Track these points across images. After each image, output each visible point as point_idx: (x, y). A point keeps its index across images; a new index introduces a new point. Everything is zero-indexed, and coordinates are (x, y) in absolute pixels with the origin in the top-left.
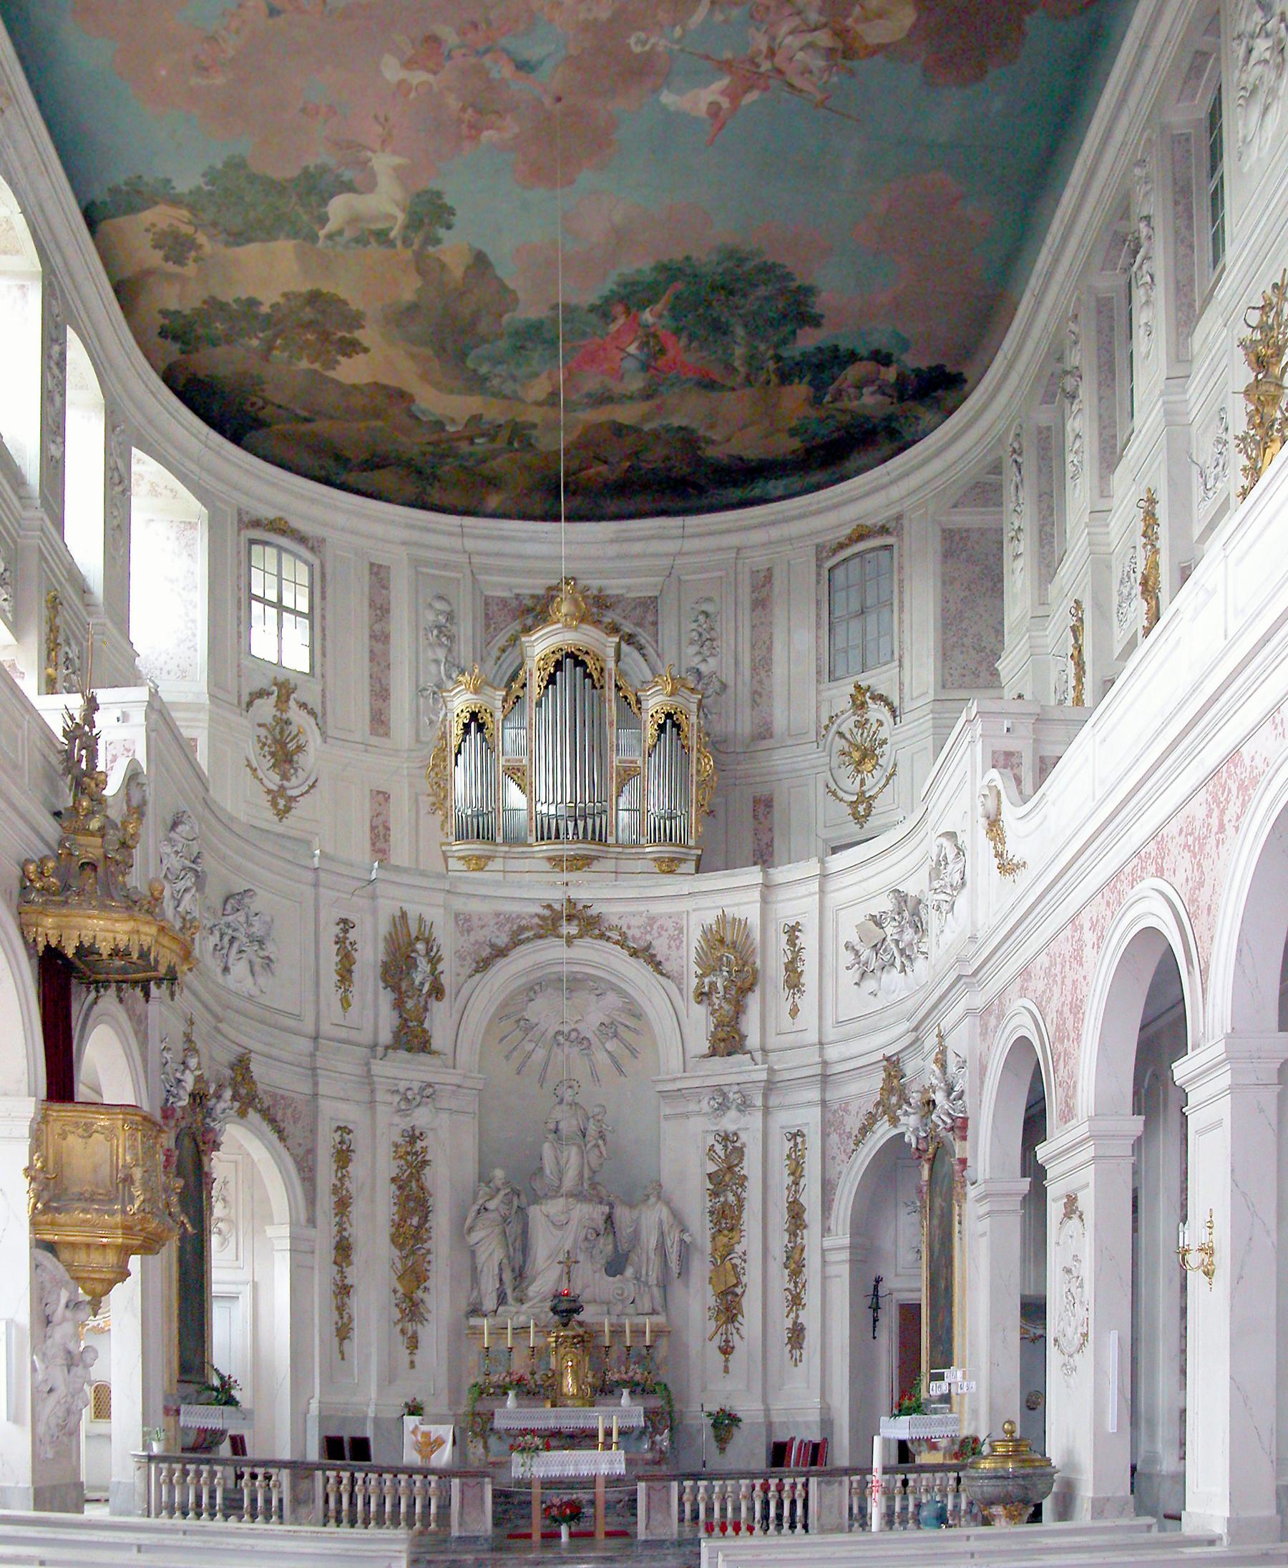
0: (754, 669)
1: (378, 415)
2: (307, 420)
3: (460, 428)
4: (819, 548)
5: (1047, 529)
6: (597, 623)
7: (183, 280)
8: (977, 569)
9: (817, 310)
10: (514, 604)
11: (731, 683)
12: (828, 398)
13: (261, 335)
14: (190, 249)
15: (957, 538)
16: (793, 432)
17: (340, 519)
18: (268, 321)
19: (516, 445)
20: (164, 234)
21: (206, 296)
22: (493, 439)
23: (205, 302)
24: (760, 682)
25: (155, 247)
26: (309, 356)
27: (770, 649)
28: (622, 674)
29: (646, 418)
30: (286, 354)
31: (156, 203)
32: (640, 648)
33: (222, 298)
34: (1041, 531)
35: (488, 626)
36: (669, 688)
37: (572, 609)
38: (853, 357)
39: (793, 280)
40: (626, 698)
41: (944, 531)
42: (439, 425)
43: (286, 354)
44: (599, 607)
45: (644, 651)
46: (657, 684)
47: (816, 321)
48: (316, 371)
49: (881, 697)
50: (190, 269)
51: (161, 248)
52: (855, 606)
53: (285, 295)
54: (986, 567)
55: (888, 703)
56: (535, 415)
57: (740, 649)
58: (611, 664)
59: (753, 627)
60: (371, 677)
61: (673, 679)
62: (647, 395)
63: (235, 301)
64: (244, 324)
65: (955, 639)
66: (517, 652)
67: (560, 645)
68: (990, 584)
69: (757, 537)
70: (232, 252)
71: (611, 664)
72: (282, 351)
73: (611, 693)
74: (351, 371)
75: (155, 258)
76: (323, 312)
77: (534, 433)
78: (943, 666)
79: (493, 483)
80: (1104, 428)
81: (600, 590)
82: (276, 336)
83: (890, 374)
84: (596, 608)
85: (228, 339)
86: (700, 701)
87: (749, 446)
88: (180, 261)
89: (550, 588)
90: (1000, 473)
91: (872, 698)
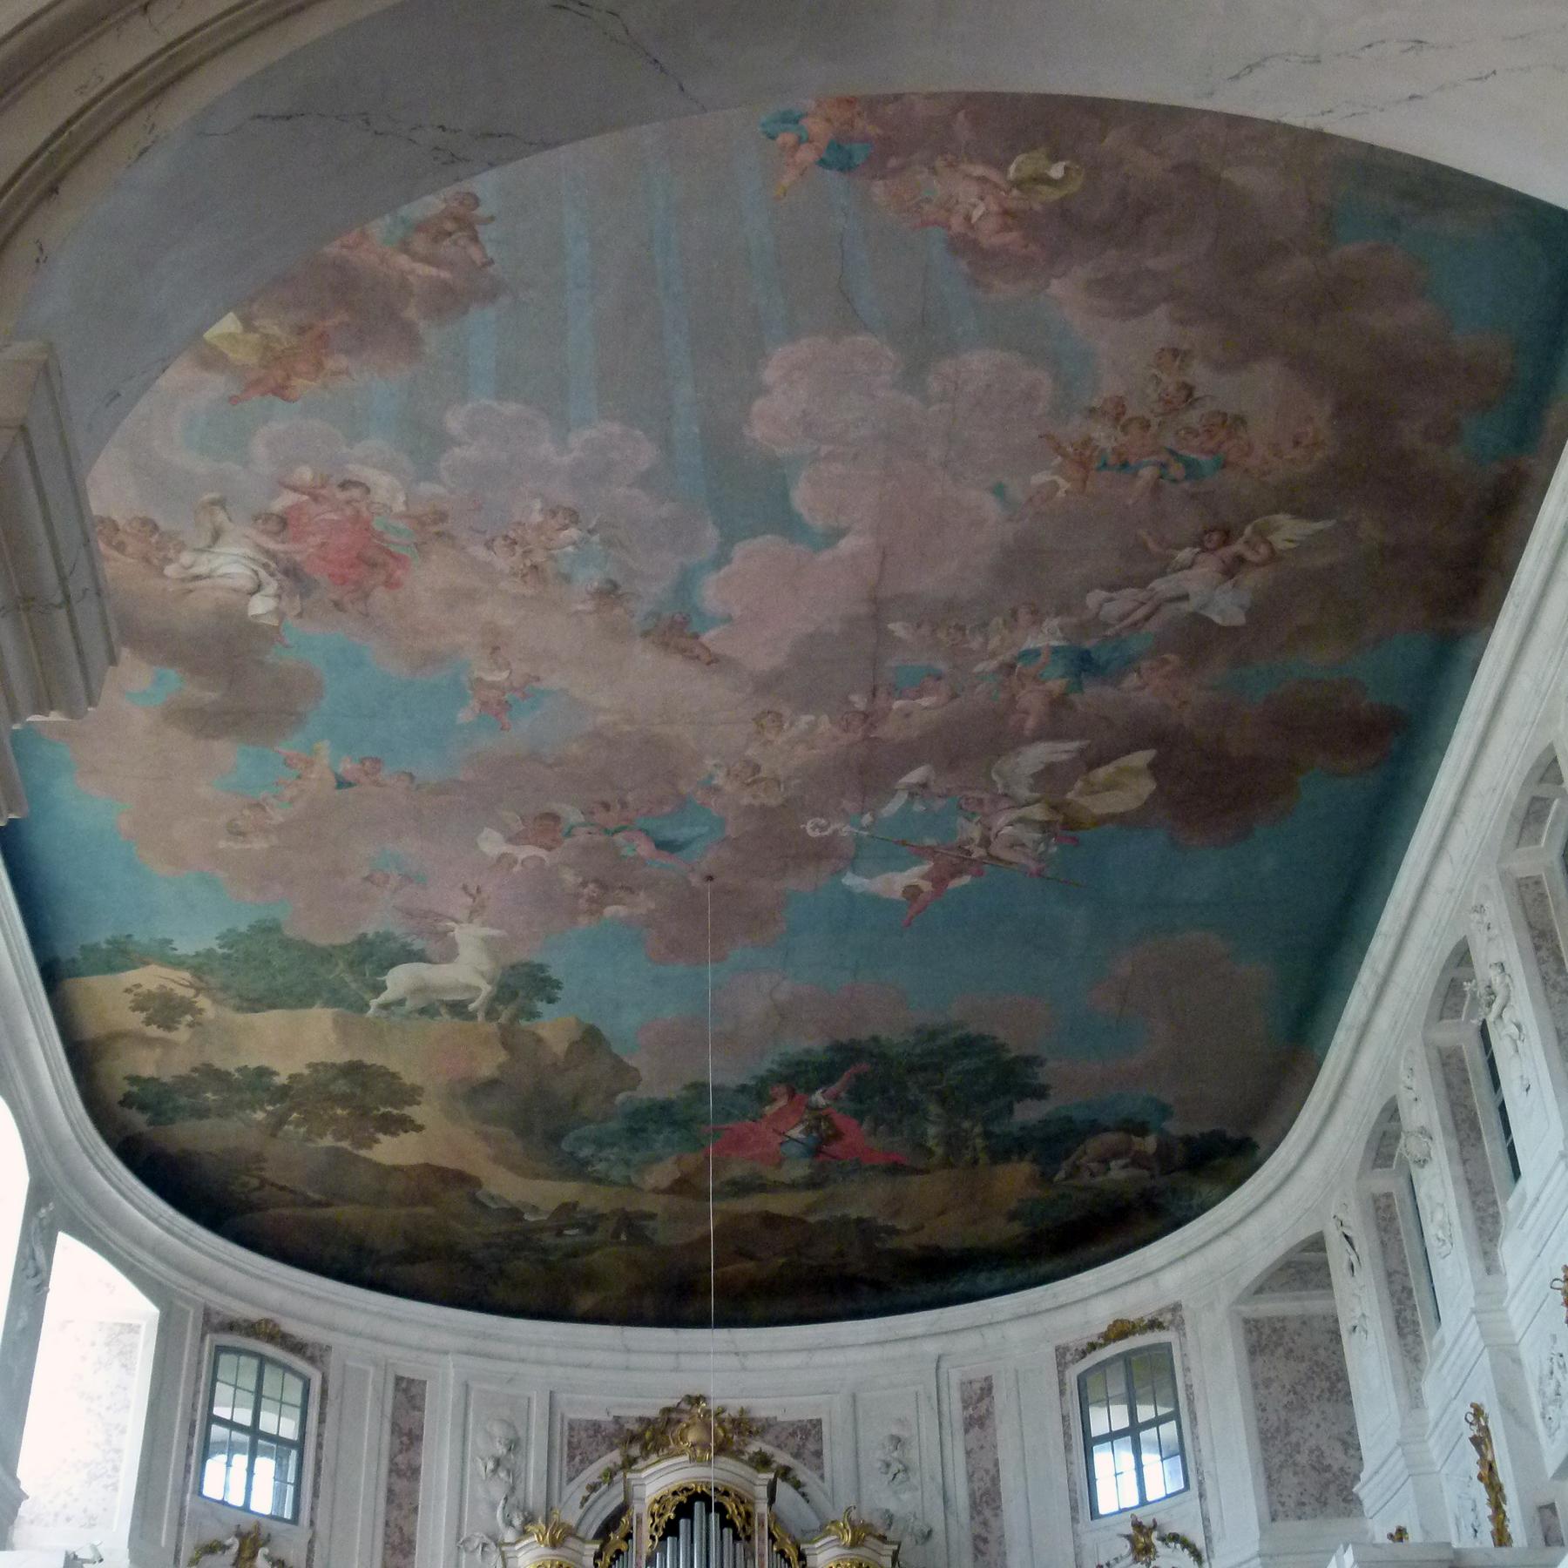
0: (975, 1507)
1: (426, 1199)
2: (328, 1205)
3: (545, 1218)
4: (1063, 1356)
5: (1408, 1314)
6: (737, 1455)
7: (166, 1044)
8: (1304, 1366)
9: (1043, 1076)
10: (612, 1428)
11: (938, 1527)
12: (1061, 1175)
13: (270, 1108)
14: (185, 1013)
15: (1267, 1331)
16: (1013, 1216)
17: (361, 1322)
18: (283, 1093)
19: (623, 1238)
20: (150, 995)
21: (197, 1064)
22: (591, 1230)
23: (195, 1070)
24: (985, 1523)
25: (134, 1010)
26: (334, 1134)
27: (995, 1480)
28: (776, 1519)
29: (811, 1209)
30: (302, 1130)
31: (146, 964)
32: (797, 1485)
33: (218, 1064)
34: (1397, 1318)
35: (571, 1458)
36: (848, 1538)
37: (704, 1437)
38: (1095, 1128)
39: (1008, 1051)
40: (782, 1553)
41: (1246, 1321)
42: (514, 1213)
43: (302, 1130)
44: (740, 1433)
45: (805, 1490)
46: (829, 1533)
47: (1040, 1093)
48: (345, 1150)
49: (1175, 1538)
50: (182, 1034)
51: (143, 1009)
52: (1120, 1419)
53: (309, 1066)
54: (1317, 1363)
55: (1186, 1544)
56: (649, 1204)
57: (949, 1481)
58: (762, 1508)
59: (968, 1453)
60: (387, 1524)
61: (853, 1527)
62: (812, 1184)
63: (239, 1070)
64: (248, 1096)
65: (1282, 1457)
66: (618, 1489)
67: (683, 1483)
68: (1326, 1385)
69: (972, 1340)
70: (241, 1018)
71: (762, 1508)
72: (298, 1125)
73: (761, 1544)
74: (390, 1150)
75: (134, 1021)
76: (364, 1086)
77: (651, 1224)
78: (1269, 1494)
79: (589, 1280)
80: (1477, 1194)
81: (742, 1411)
82: (291, 1110)
83: (1150, 1144)
84: (733, 1434)
85: (223, 1112)
86: (896, 1553)
87: (951, 1232)
88: (169, 1025)
89: (667, 1410)
90: (1323, 1249)
91: (1163, 1539)
